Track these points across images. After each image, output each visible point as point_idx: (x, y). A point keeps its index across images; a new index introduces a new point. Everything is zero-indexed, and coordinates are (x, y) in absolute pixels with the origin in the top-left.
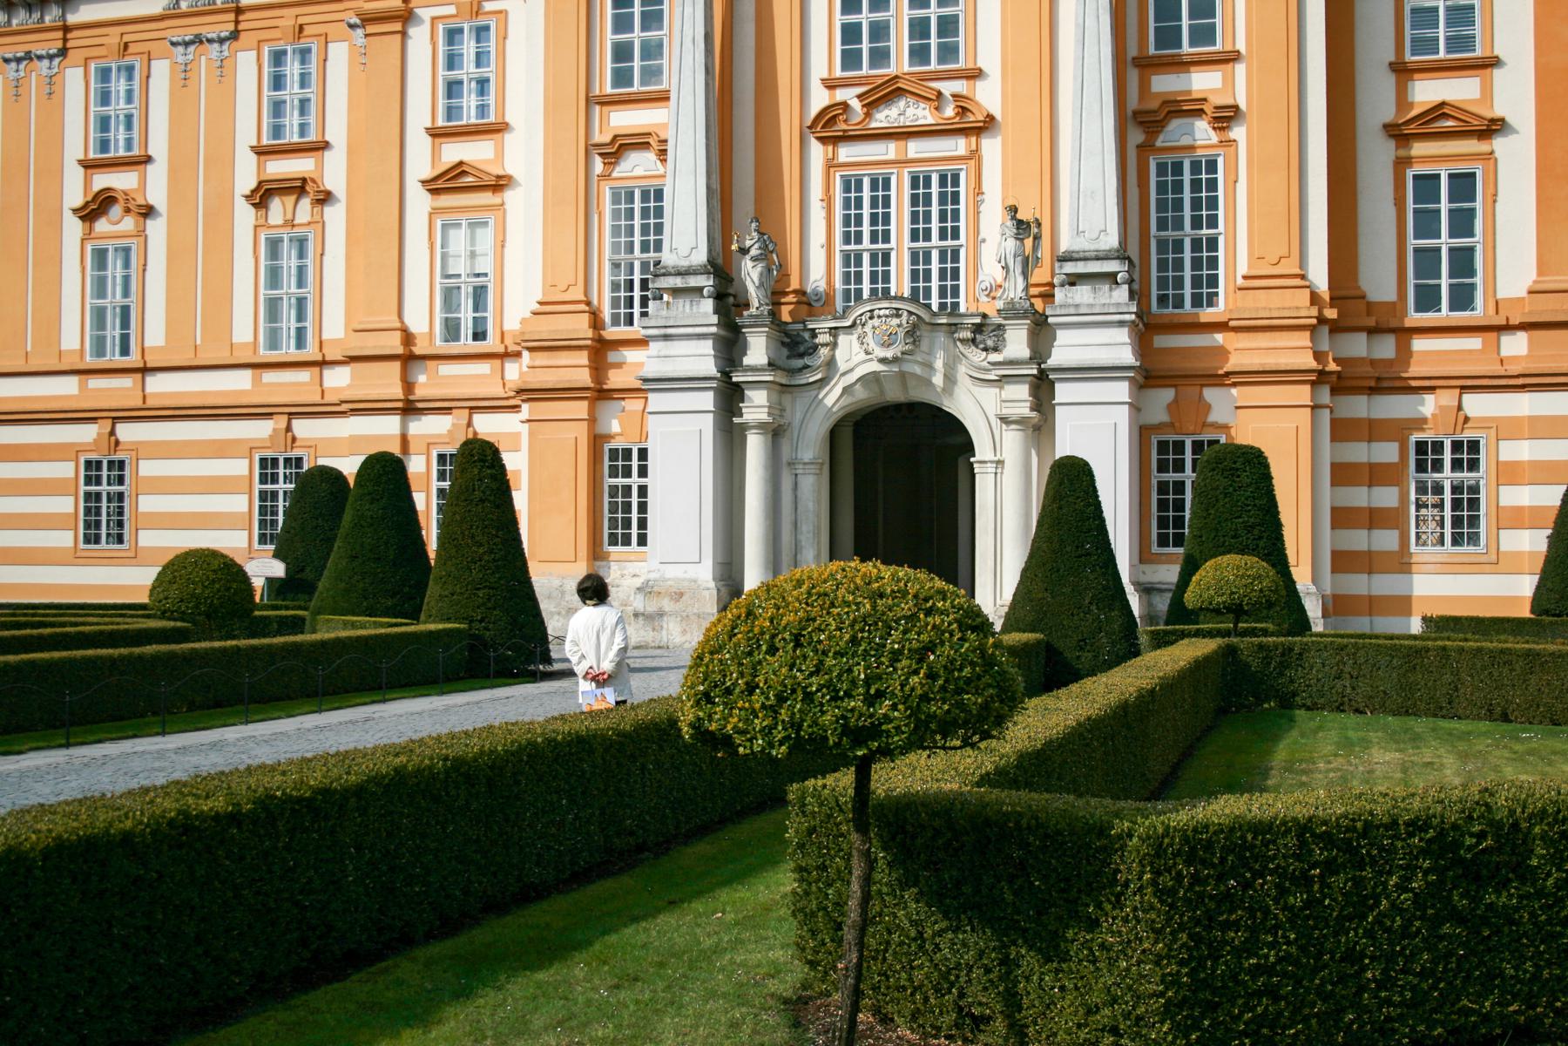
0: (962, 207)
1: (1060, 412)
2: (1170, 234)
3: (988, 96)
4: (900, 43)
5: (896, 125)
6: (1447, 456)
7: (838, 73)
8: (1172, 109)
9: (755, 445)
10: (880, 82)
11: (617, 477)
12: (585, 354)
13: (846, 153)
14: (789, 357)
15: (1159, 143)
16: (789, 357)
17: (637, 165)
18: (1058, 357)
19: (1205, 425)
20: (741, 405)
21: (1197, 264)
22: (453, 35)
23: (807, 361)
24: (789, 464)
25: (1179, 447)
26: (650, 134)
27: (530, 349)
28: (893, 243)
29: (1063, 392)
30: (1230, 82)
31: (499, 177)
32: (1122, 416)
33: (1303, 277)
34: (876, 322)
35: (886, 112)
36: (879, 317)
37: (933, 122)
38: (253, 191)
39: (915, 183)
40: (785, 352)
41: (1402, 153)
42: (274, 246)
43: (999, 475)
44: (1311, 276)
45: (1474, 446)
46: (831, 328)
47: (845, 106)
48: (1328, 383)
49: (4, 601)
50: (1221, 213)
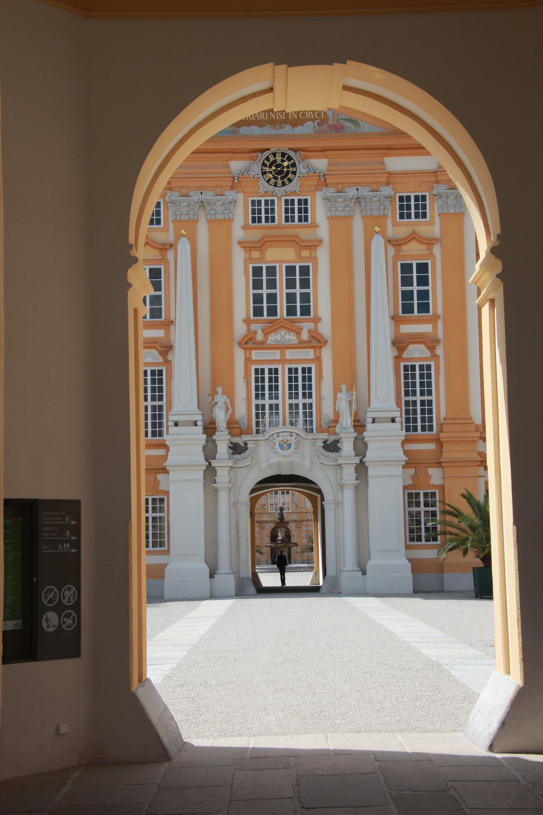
0: (313, 383)
2: (411, 398)
4: (282, 305)
8: (411, 341)
9: (223, 497)
13: (255, 355)
14: (232, 454)
15: (404, 356)
16: (232, 454)
20: (216, 477)
21: (423, 412)
25: (418, 495)
26: (157, 343)
30: (435, 328)
33: (470, 418)
35: (275, 337)
39: (290, 370)
46: (254, 440)
50: (433, 388)
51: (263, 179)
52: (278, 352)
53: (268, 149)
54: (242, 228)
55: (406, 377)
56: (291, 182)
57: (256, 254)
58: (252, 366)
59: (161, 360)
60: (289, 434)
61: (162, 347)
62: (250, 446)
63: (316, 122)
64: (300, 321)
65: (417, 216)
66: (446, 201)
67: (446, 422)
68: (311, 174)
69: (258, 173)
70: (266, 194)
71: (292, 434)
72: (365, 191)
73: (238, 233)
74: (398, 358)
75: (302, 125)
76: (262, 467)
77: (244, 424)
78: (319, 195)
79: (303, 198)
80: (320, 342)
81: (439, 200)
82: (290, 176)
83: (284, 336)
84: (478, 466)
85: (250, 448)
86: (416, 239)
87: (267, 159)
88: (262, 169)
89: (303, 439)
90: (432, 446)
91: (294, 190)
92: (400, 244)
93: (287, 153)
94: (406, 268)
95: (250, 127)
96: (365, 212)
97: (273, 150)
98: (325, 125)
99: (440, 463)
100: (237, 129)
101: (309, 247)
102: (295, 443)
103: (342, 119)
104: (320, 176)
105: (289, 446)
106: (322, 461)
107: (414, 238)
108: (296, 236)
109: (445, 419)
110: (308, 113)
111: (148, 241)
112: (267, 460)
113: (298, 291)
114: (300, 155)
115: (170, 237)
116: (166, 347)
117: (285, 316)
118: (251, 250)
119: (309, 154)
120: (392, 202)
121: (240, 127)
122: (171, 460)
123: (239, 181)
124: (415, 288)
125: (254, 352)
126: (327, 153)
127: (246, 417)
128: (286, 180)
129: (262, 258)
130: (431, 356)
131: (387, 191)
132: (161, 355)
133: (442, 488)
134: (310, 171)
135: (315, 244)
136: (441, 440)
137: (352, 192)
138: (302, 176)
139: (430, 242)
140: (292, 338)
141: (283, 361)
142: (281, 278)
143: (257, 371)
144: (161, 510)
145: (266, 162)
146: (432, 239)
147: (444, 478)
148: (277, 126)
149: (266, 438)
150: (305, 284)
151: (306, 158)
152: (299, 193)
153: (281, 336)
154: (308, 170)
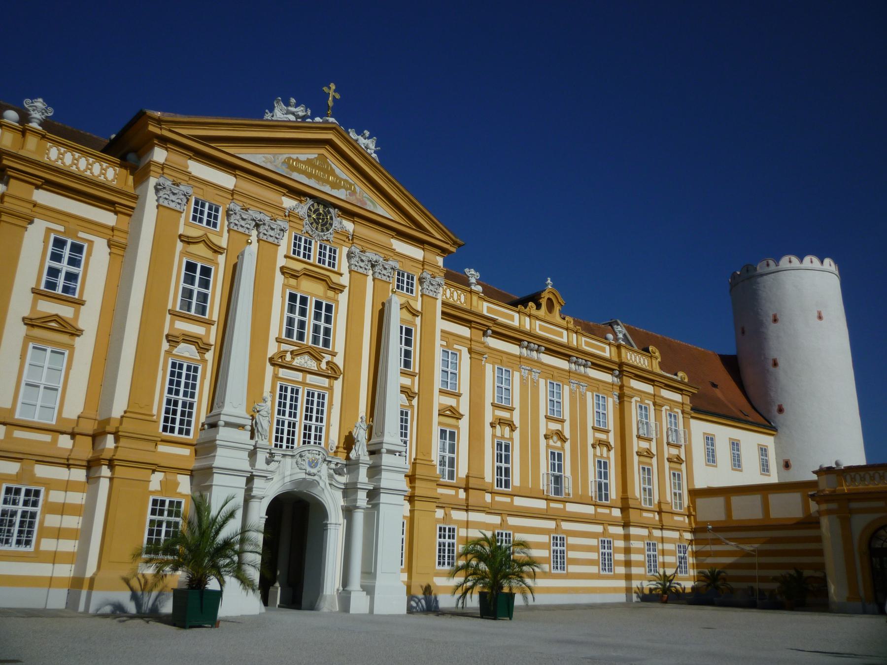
10: (304, 347)
11: (172, 516)
13: (282, 372)
22: (59, 243)
28: (298, 419)
29: (384, 498)
35: (300, 360)
37: (317, 369)
46: (282, 454)
47: (287, 352)
52: (300, 374)
54: (286, 257)
57: (293, 282)
59: (199, 358)
63: (348, 191)
71: (320, 453)
75: (339, 190)
88: (308, 212)
98: (354, 197)
100: (291, 172)
103: (365, 197)
112: (290, 475)
113: (322, 324)
117: (310, 344)
121: (293, 172)
123: (289, 216)
129: (296, 288)
140: (312, 365)
141: (304, 383)
142: (311, 308)
143: (281, 387)
145: (312, 208)
150: (328, 320)
151: (339, 216)
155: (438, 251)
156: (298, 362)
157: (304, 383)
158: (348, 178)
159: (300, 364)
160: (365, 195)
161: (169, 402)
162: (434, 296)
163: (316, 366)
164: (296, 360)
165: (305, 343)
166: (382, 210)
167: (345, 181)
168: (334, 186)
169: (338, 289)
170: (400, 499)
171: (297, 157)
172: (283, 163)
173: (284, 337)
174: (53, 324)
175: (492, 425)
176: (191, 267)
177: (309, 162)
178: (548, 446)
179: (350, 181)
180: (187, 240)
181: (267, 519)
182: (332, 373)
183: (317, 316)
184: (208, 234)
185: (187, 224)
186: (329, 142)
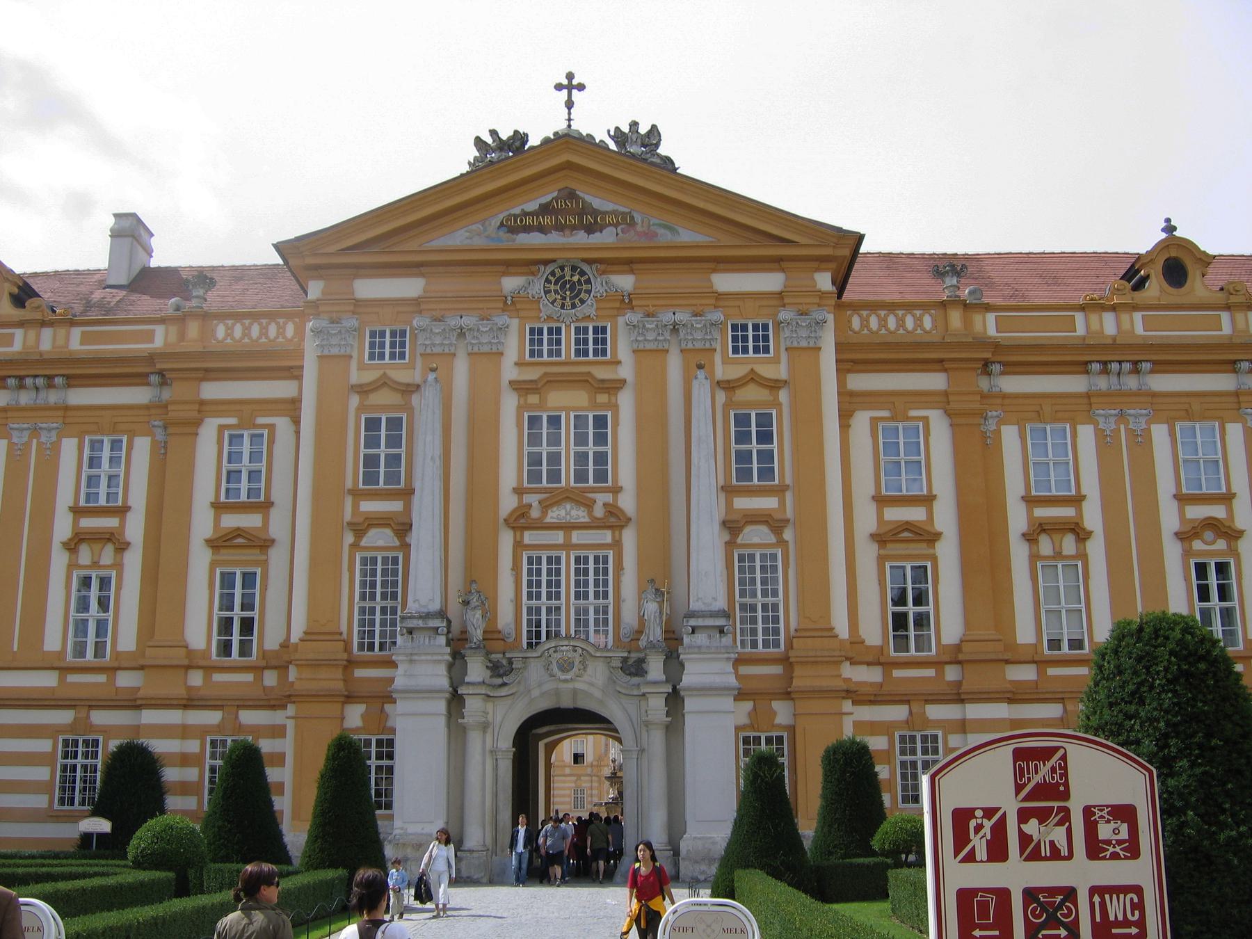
1: (687, 717)
2: (748, 600)
3: (627, 502)
4: (568, 469)
5: (564, 521)
6: (919, 745)
7: (526, 484)
12: (340, 670)
13: (529, 537)
15: (739, 541)
16: (491, 677)
17: (380, 538)
18: (688, 679)
19: (773, 726)
21: (765, 620)
23: (505, 679)
24: (492, 752)
26: (392, 519)
27: (297, 665)
29: (690, 704)
30: (782, 503)
31: (265, 540)
32: (730, 723)
33: (832, 629)
34: (558, 655)
35: (557, 513)
36: (562, 651)
38: (70, 540)
39: (578, 560)
40: (489, 673)
41: (882, 552)
42: (86, 582)
43: (639, 760)
44: (837, 631)
45: (935, 738)
48: (851, 698)
49: (4, 851)
51: (546, 300)
53: (554, 261)
55: (741, 570)
56: (584, 303)
57: (533, 399)
58: (524, 553)
59: (398, 543)
60: (571, 648)
61: (398, 524)
62: (517, 666)
63: (619, 229)
64: (593, 490)
65: (756, 350)
66: (796, 331)
67: (798, 634)
68: (612, 293)
69: (538, 292)
70: (549, 318)
71: (576, 648)
72: (683, 316)
73: (509, 372)
74: (730, 545)
76: (533, 697)
77: (510, 634)
78: (621, 320)
79: (600, 324)
80: (620, 519)
81: (785, 328)
82: (582, 295)
83: (570, 511)
84: (844, 698)
85: (516, 669)
86: (754, 380)
87: (553, 273)
88: (544, 287)
89: (592, 656)
90: (777, 670)
91: (587, 314)
92: (733, 387)
93: (580, 265)
94: (743, 420)
95: (531, 234)
96: (685, 343)
97: (560, 263)
98: (632, 232)
99: (789, 693)
100: (515, 236)
101: (607, 391)
102: (580, 662)
103: (654, 225)
104: (623, 296)
105: (571, 665)
106: (619, 689)
107: (752, 378)
108: (589, 374)
109: (796, 630)
110: (609, 217)
111: (386, 381)
114: (597, 266)
115: (415, 376)
116: (404, 524)
117: (572, 484)
118: (527, 394)
119: (610, 268)
120: (723, 332)
122: (400, 682)
124: (754, 446)
125: (527, 534)
126: (635, 266)
127: (513, 626)
128: (577, 301)
129: (541, 406)
130: (777, 542)
131: (718, 316)
132: (397, 536)
133: (792, 729)
134: (610, 289)
135: (615, 386)
136: (791, 660)
137: (667, 317)
138: (599, 295)
139: (774, 385)
140: (579, 515)
141: (568, 546)
142: (567, 430)
144: (390, 756)
145: (550, 278)
146: (777, 381)
147: (794, 715)
148: (567, 232)
149: (539, 655)
150: (601, 439)
151: (604, 272)
152: (595, 318)
153: (566, 511)
154: (607, 288)
155: (815, 265)
156: (554, 515)
157: (568, 546)
158: (616, 207)
159: (558, 519)
160: (653, 221)
161: (362, 611)
162: (812, 344)
163: (586, 516)
164: (550, 514)
165: (563, 484)
166: (688, 236)
167: (614, 212)
168: (590, 230)
169: (615, 386)
170: (728, 703)
171: (523, 210)
172: (499, 228)
173: (526, 484)
174: (240, 541)
175: (1030, 538)
176: (372, 424)
177: (545, 209)
178: (1187, 553)
179: (622, 209)
180: (363, 390)
181: (514, 754)
182: (615, 519)
183: (581, 439)
184: (387, 371)
185: (362, 367)
186: (569, 166)
